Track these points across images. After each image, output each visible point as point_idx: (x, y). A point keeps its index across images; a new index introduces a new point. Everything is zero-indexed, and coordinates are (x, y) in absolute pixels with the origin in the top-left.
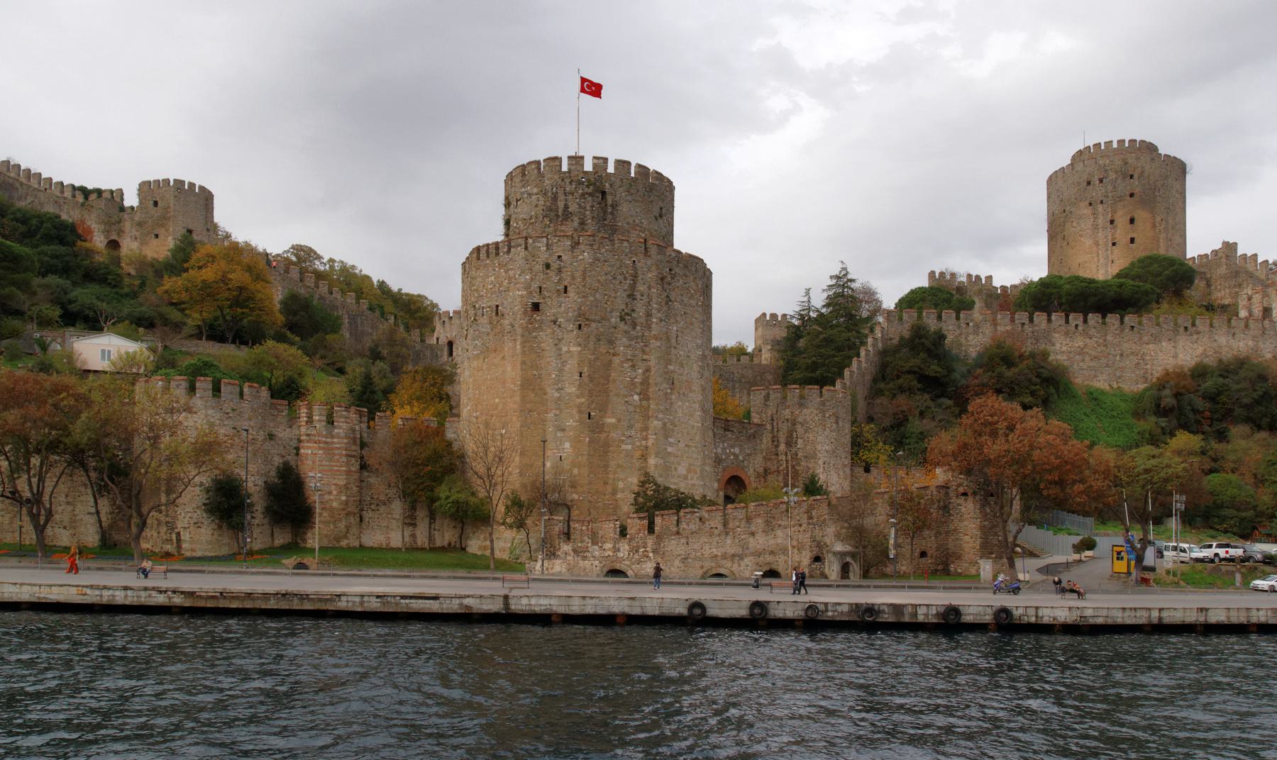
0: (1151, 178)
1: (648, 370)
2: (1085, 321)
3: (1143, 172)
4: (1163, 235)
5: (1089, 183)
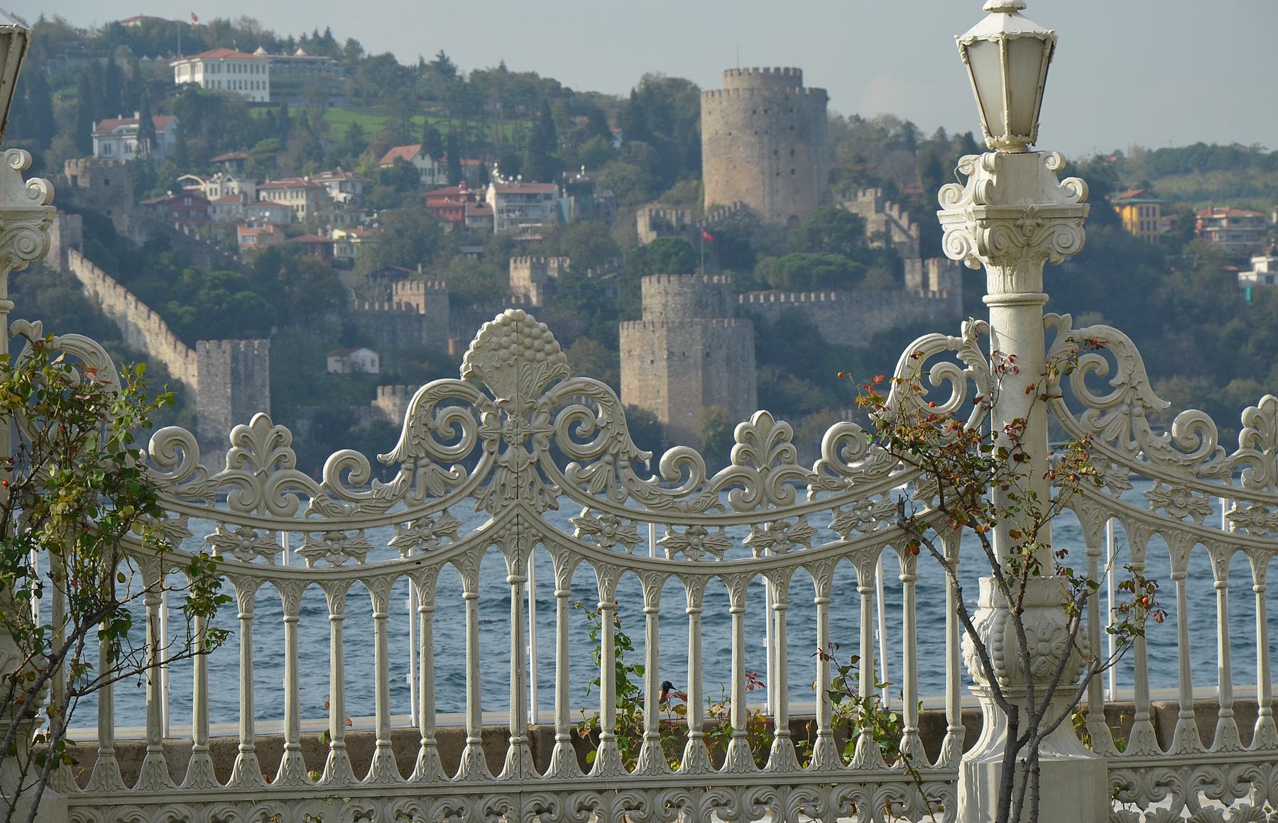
5: (755, 112)
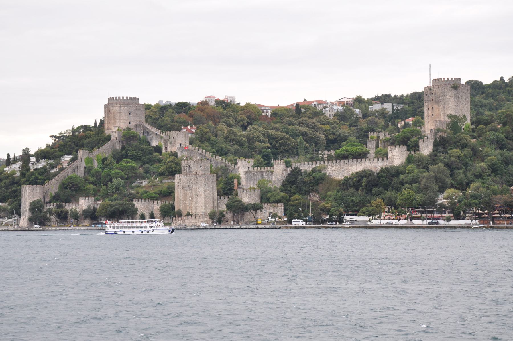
0: (438, 93)
1: (192, 194)
2: (336, 162)
3: (435, 92)
4: (442, 112)
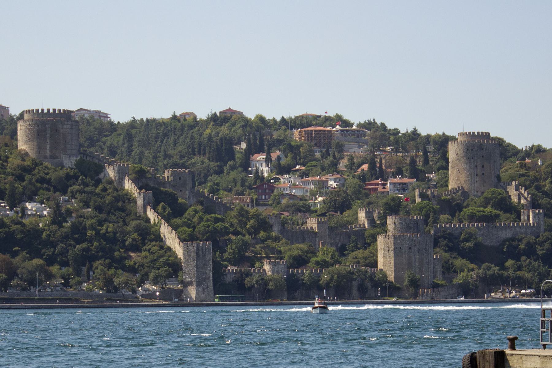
4: (493, 172)
5: (468, 150)
